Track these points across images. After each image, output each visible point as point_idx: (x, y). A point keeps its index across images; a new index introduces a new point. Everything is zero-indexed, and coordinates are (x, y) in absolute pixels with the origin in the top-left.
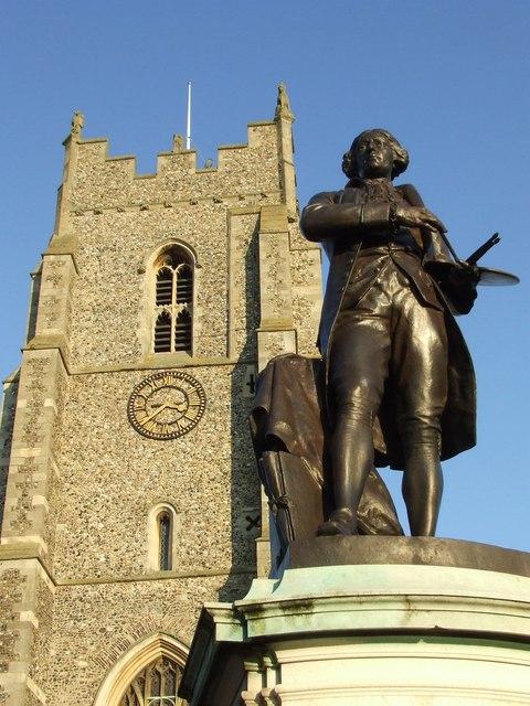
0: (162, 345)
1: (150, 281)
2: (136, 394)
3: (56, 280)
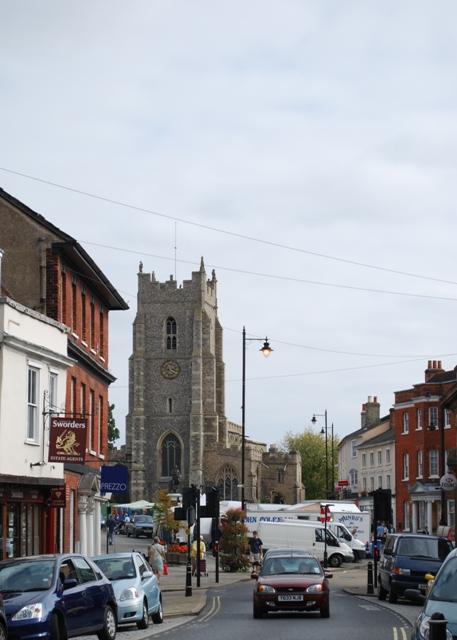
0: (169, 347)
1: (164, 329)
2: (162, 367)
3: (140, 332)
